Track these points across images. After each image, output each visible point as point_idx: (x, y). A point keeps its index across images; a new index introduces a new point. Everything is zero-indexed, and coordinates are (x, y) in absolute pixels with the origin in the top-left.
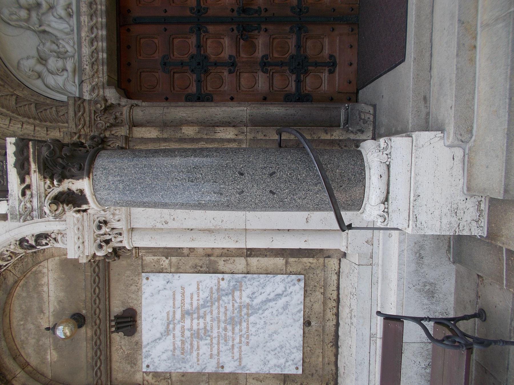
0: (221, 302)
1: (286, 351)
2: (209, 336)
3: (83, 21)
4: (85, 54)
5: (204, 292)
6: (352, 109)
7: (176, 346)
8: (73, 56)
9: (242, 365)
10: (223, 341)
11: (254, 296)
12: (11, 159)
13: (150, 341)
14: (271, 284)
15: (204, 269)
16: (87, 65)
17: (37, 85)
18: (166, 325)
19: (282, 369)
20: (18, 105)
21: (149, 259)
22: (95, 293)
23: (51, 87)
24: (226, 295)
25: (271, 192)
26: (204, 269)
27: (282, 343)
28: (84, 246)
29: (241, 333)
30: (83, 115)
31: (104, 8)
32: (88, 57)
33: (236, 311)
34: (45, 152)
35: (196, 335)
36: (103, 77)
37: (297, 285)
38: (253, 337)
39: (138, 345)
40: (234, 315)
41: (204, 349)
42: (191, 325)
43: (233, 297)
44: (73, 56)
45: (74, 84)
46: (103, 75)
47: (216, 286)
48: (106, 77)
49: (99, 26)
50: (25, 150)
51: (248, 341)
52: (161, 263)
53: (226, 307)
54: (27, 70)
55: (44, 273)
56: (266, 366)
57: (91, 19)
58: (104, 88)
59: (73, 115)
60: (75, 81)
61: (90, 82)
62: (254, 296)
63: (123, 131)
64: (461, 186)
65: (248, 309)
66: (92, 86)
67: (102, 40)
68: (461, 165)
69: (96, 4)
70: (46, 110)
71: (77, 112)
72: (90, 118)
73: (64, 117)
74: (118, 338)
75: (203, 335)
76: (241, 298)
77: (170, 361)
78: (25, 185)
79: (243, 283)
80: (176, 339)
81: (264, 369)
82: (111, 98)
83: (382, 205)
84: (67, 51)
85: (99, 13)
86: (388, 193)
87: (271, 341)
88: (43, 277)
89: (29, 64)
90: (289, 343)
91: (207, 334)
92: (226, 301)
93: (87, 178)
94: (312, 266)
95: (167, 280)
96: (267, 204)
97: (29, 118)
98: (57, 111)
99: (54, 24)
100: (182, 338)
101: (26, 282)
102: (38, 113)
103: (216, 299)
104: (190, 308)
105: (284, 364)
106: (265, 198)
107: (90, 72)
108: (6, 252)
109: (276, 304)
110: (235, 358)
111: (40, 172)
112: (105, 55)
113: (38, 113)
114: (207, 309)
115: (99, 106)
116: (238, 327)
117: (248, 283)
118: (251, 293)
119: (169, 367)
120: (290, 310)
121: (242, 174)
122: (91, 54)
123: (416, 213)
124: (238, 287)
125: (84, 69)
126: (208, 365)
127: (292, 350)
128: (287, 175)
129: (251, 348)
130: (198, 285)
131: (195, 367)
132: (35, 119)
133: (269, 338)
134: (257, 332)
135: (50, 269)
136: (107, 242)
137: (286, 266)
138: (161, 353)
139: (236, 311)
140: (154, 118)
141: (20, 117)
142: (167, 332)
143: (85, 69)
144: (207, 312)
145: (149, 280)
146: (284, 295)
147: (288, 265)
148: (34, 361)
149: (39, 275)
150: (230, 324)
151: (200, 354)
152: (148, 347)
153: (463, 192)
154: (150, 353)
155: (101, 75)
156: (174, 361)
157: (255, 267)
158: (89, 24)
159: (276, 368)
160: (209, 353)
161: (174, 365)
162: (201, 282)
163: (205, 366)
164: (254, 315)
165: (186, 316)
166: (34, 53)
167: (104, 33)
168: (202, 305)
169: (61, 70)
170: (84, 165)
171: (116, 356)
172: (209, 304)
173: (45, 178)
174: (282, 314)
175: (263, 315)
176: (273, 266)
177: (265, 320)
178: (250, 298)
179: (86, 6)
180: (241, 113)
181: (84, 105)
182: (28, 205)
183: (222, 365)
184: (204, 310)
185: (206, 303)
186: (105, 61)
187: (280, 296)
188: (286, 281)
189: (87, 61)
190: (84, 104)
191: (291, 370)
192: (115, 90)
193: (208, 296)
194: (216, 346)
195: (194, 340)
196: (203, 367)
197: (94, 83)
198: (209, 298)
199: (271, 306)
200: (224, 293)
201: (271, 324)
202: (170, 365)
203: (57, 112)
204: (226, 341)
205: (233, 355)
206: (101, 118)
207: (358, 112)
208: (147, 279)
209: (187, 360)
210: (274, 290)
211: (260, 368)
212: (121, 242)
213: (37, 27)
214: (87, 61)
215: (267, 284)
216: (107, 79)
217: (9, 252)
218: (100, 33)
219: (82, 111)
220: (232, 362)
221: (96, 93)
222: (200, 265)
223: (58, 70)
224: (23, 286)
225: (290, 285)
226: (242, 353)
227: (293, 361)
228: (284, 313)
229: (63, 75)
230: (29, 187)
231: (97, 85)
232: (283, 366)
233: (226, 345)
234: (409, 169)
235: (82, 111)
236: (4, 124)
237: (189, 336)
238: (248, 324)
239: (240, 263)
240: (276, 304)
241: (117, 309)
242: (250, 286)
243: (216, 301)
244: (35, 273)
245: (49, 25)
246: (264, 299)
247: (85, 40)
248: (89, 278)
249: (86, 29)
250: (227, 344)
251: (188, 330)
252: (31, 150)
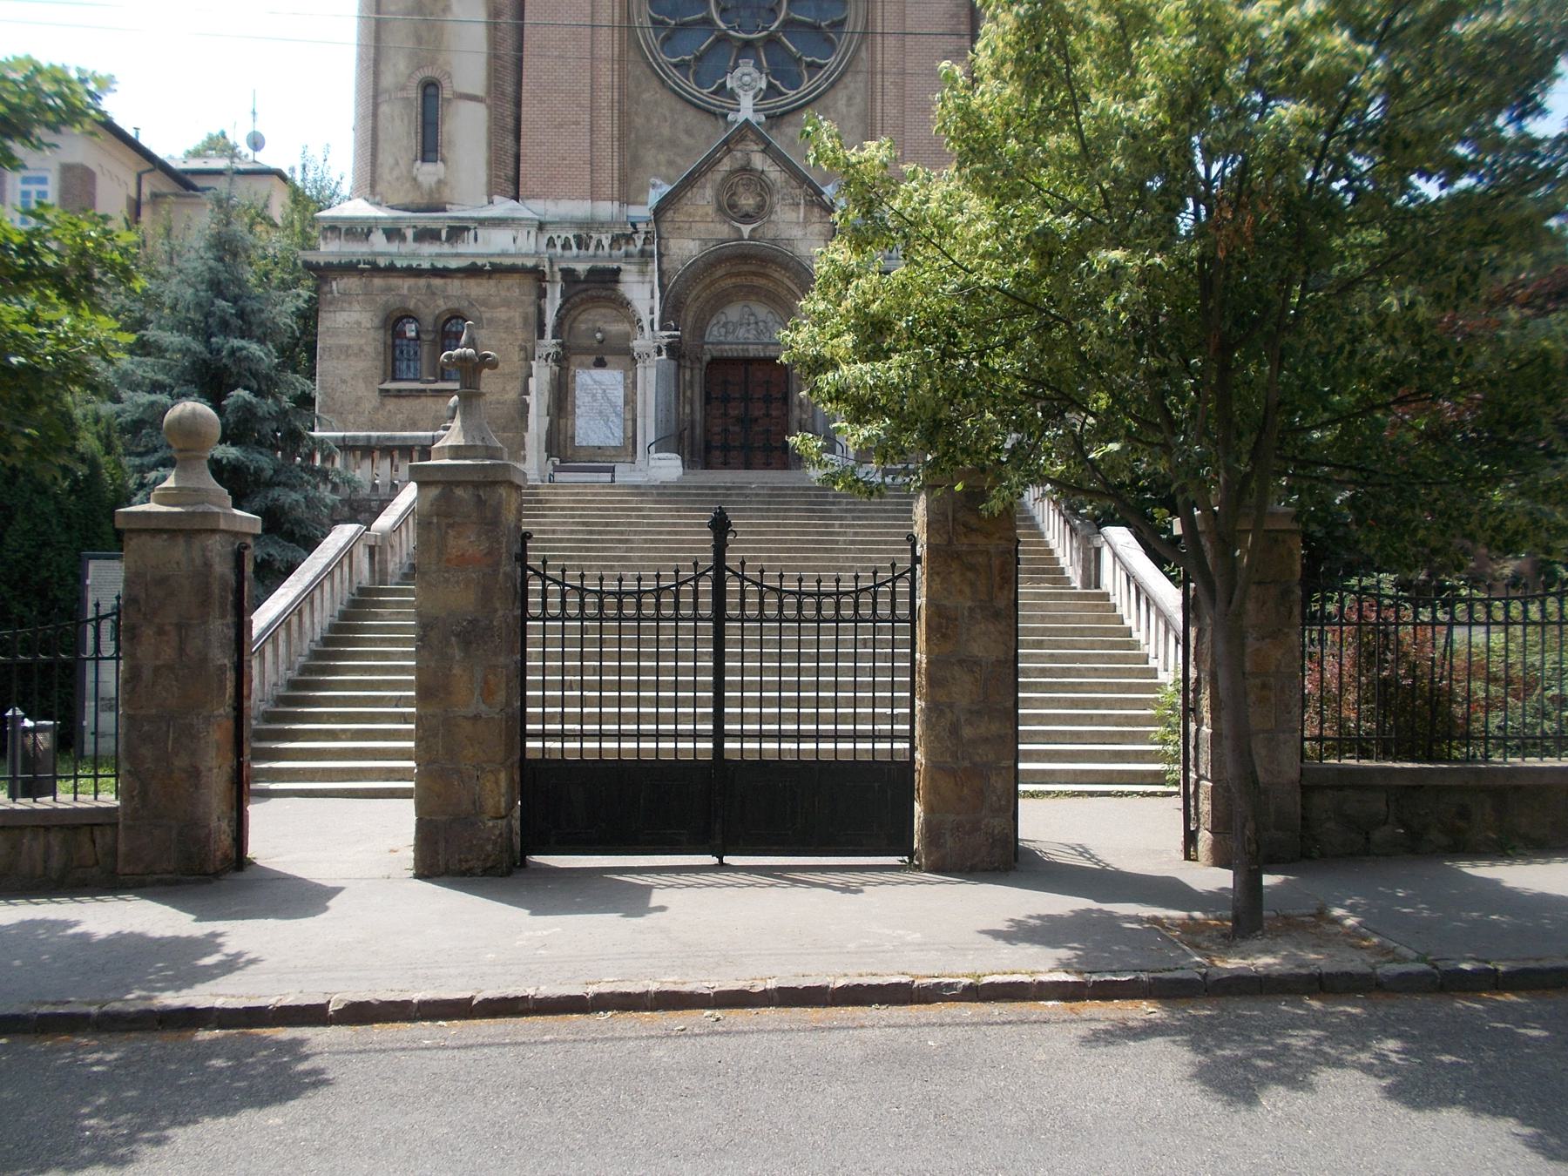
17: (714, 321)
21: (631, 374)
36: (715, 354)
39: (588, 368)
41: (587, 399)
63: (688, 364)
74: (593, 358)
89: (723, 319)
124: (617, 415)
142: (595, 382)
148: (582, 318)
171: (583, 357)
191: (577, 440)
239: (629, 416)
241: (607, 358)
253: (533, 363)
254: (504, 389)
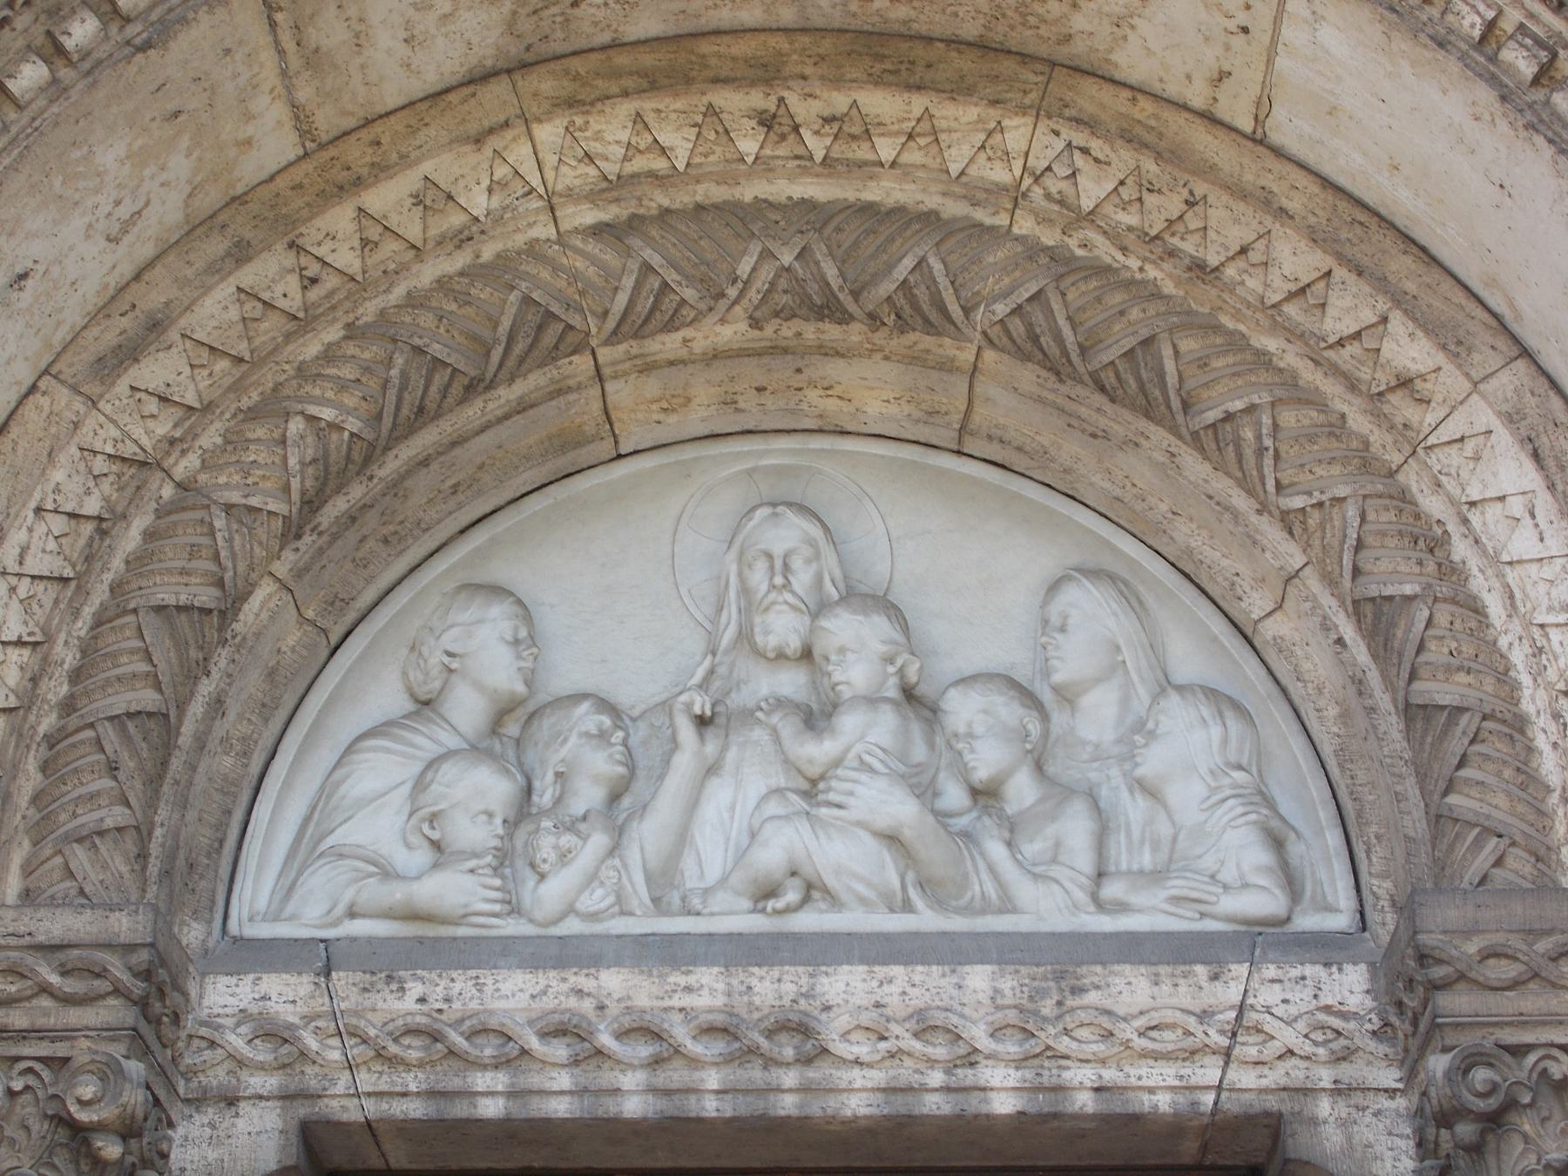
3: (691, 980)
4: (489, 989)
8: (514, 908)
16: (422, 1000)
20: (150, 622)
23: (337, 775)
30: (45, 989)
31: (787, 1105)
32: (474, 1005)
44: (514, 908)
45: (340, 909)
46: (369, 1094)
48: (351, 1112)
49: (675, 1075)
54: (449, 640)
57: (710, 1030)
58: (287, 1097)
59: (41, 938)
60: (364, 916)
61: (319, 1016)
66: (291, 1027)
67: (585, 1090)
69: (806, 1061)
70: (113, 769)
72: (23, 1035)
73: (56, 876)
82: (220, 1143)
84: (542, 877)
85: (755, 1074)
97: (76, 676)
98: (101, 833)
99: (719, 794)
102: (91, 726)
107: (378, 1019)
112: (491, 1108)
113: (91, 726)
115: (88, 1091)
122: (493, 1023)
125: (401, 981)
132: (68, 706)
141: (82, 627)
143: (402, 989)
155: (366, 1081)
158: (677, 1018)
166: (567, 675)
167: (633, 1107)
169: (435, 835)
179: (786, 1002)
181: (102, 997)
186: (460, 1110)
189: (448, 1000)
190: (112, 1001)
192: (273, 1166)
197: (312, 1043)
203: (90, 838)
206: (28, 1097)
213: (689, 706)
214: (448, 1000)
216: (345, 1117)
218: (631, 1080)
219: (71, 986)
221: (246, 1051)
223: (433, 819)
229: (408, 846)
231: (303, 1055)
235: (71, 986)
236: (24, 550)
245: (712, 770)
247: (579, 992)
249: (642, 1001)
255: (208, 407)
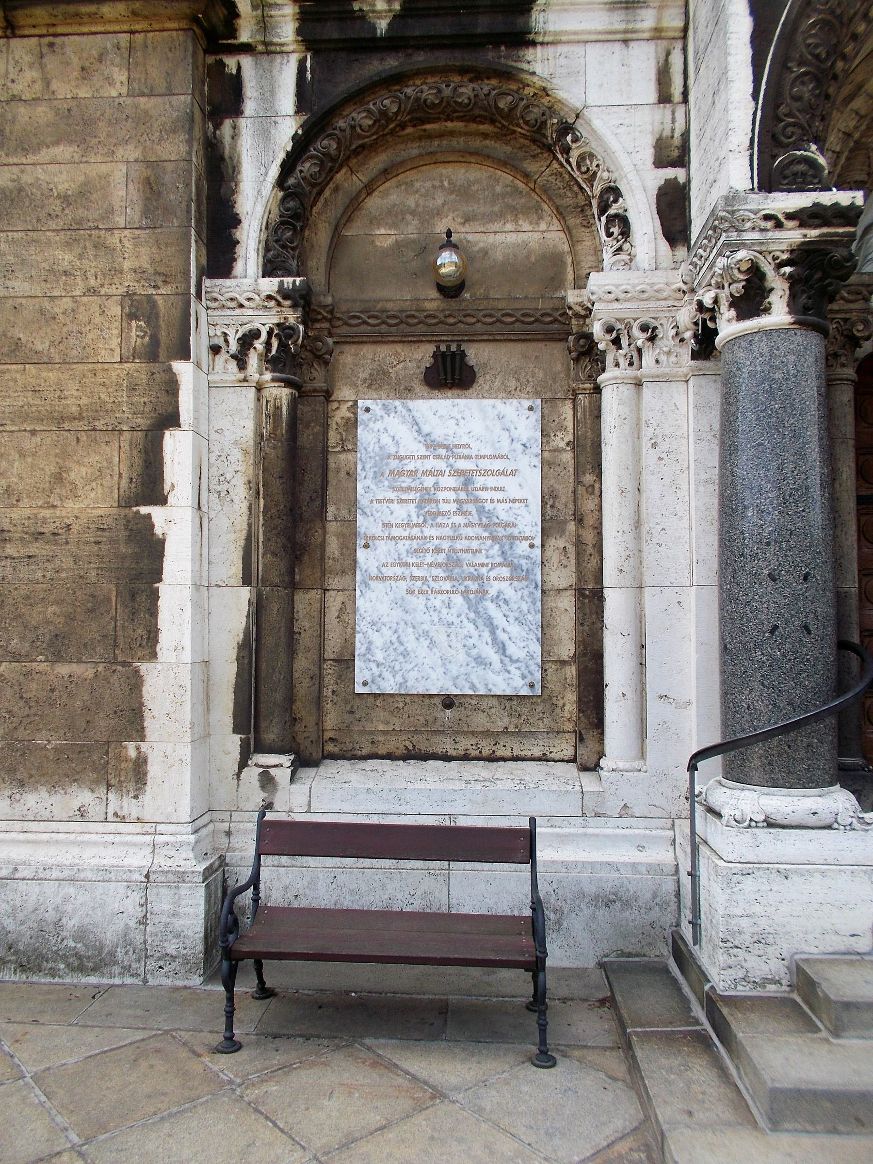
0: (489, 542)
1: (397, 663)
2: (425, 521)
5: (507, 511)
6: (864, 777)
7: (406, 461)
9: (371, 582)
10: (416, 547)
11: (501, 603)
12: (827, 198)
13: (415, 413)
14: (524, 634)
15: (549, 511)
18: (445, 442)
19: (364, 655)
22: (503, 315)
24: (503, 553)
25: (775, 627)
26: (549, 512)
27: (413, 655)
28: (611, 302)
29: (430, 579)
33: (472, 569)
34: (839, 254)
35: (427, 497)
37: (523, 682)
38: (424, 602)
39: (405, 392)
40: (465, 567)
41: (400, 513)
42: (446, 488)
43: (499, 565)
47: (520, 533)
50: (841, 221)
51: (416, 592)
52: (558, 433)
53: (480, 551)
55: (538, 224)
56: (369, 626)
62: (501, 603)
64: (806, 949)
65: (476, 592)
68: (842, 948)
71: (848, 288)
72: (837, 312)
74: (424, 354)
75: (426, 510)
76: (496, 579)
77: (377, 449)
78: (783, 220)
79: (525, 583)
80: (419, 461)
81: (365, 623)
83: (763, 818)
86: (783, 827)
87: (417, 635)
88: (531, 223)
90: (412, 669)
91: (428, 518)
92: (491, 552)
93: (792, 320)
94: (558, 710)
95: (528, 445)
96: (749, 621)
100: (420, 472)
101: (521, 192)
103: (495, 534)
104: (477, 485)
105: (373, 659)
106: (764, 617)
108: (595, 163)
109: (487, 643)
110: (384, 570)
111: (803, 243)
114: (476, 516)
115: (861, 327)
116: (442, 575)
117: (526, 592)
118: (506, 597)
119: (365, 449)
120: (475, 669)
121: (805, 578)
123: (757, 874)
124: (518, 574)
126: (371, 519)
127: (400, 674)
128: (806, 655)
129: (403, 599)
130: (520, 501)
131: (367, 495)
133: (421, 632)
134: (433, 609)
135: (545, 234)
136: (617, 342)
137: (556, 662)
138: (392, 434)
139: (472, 569)
140: (837, 422)
142: (432, 445)
144: (469, 517)
145: (528, 413)
146: (503, 658)
147: (558, 666)
148: (374, 203)
149: (535, 217)
150: (448, 559)
151: (390, 505)
152: (404, 411)
153: (796, 953)
154: (392, 414)
156: (377, 458)
157: (554, 605)
159: (366, 645)
160: (393, 522)
161: (370, 457)
162: (527, 506)
163: (369, 513)
164: (464, 603)
165: (462, 479)
168: (484, 508)
170: (810, 315)
171: (384, 352)
172: (484, 520)
173: (792, 251)
174: (468, 655)
175: (465, 621)
176: (556, 637)
177: (455, 623)
178: (498, 597)
180: (849, 577)
181: (859, 300)
182: (748, 225)
183: (371, 544)
184: (474, 512)
185: (487, 515)
187: (501, 651)
188: (531, 662)
191: (362, 672)
193: (501, 518)
194: (406, 534)
195: (418, 494)
196: (367, 511)
198: (497, 521)
199: (482, 634)
200: (507, 547)
201: (448, 636)
202: (370, 449)
204: (416, 551)
205: (389, 565)
207: (860, 788)
208: (531, 409)
209: (380, 481)
210: (514, 640)
211: (365, 615)
212: (617, 365)
215: (524, 626)
217: (595, 169)
219: (850, 297)
220: (377, 564)
222: (557, 504)
224: (515, 188)
225: (523, 668)
226: (393, 582)
227: (380, 676)
228: (470, 659)
230: (779, 225)
232: (370, 657)
233: (407, 551)
234: (829, 861)
237: (425, 485)
238: (448, 592)
240: (487, 643)
241: (475, 354)
242: (519, 596)
243: (491, 534)
244: (538, 209)
246: (495, 622)
248: (533, 306)
250: (410, 555)
251: (437, 483)
252: (841, 230)
253: (183, 369)
254: (59, 478)
255: (866, 116)
